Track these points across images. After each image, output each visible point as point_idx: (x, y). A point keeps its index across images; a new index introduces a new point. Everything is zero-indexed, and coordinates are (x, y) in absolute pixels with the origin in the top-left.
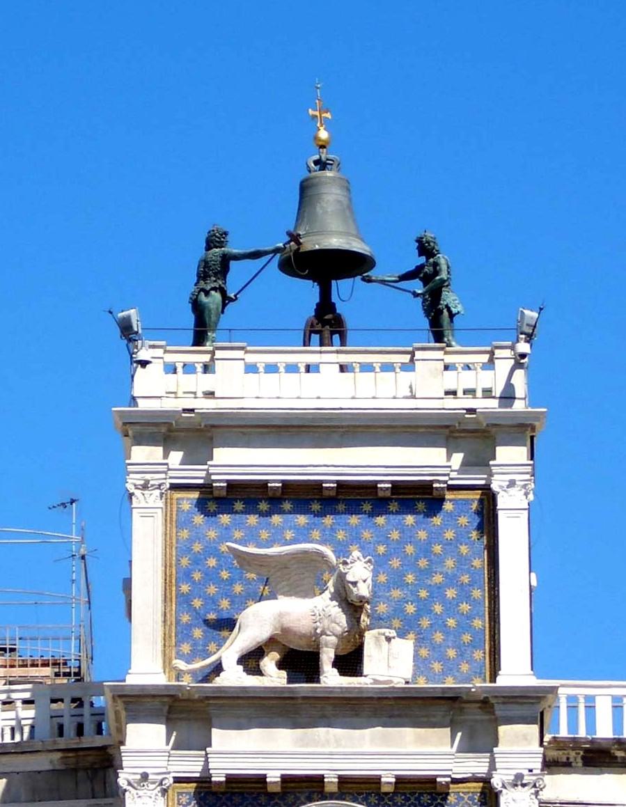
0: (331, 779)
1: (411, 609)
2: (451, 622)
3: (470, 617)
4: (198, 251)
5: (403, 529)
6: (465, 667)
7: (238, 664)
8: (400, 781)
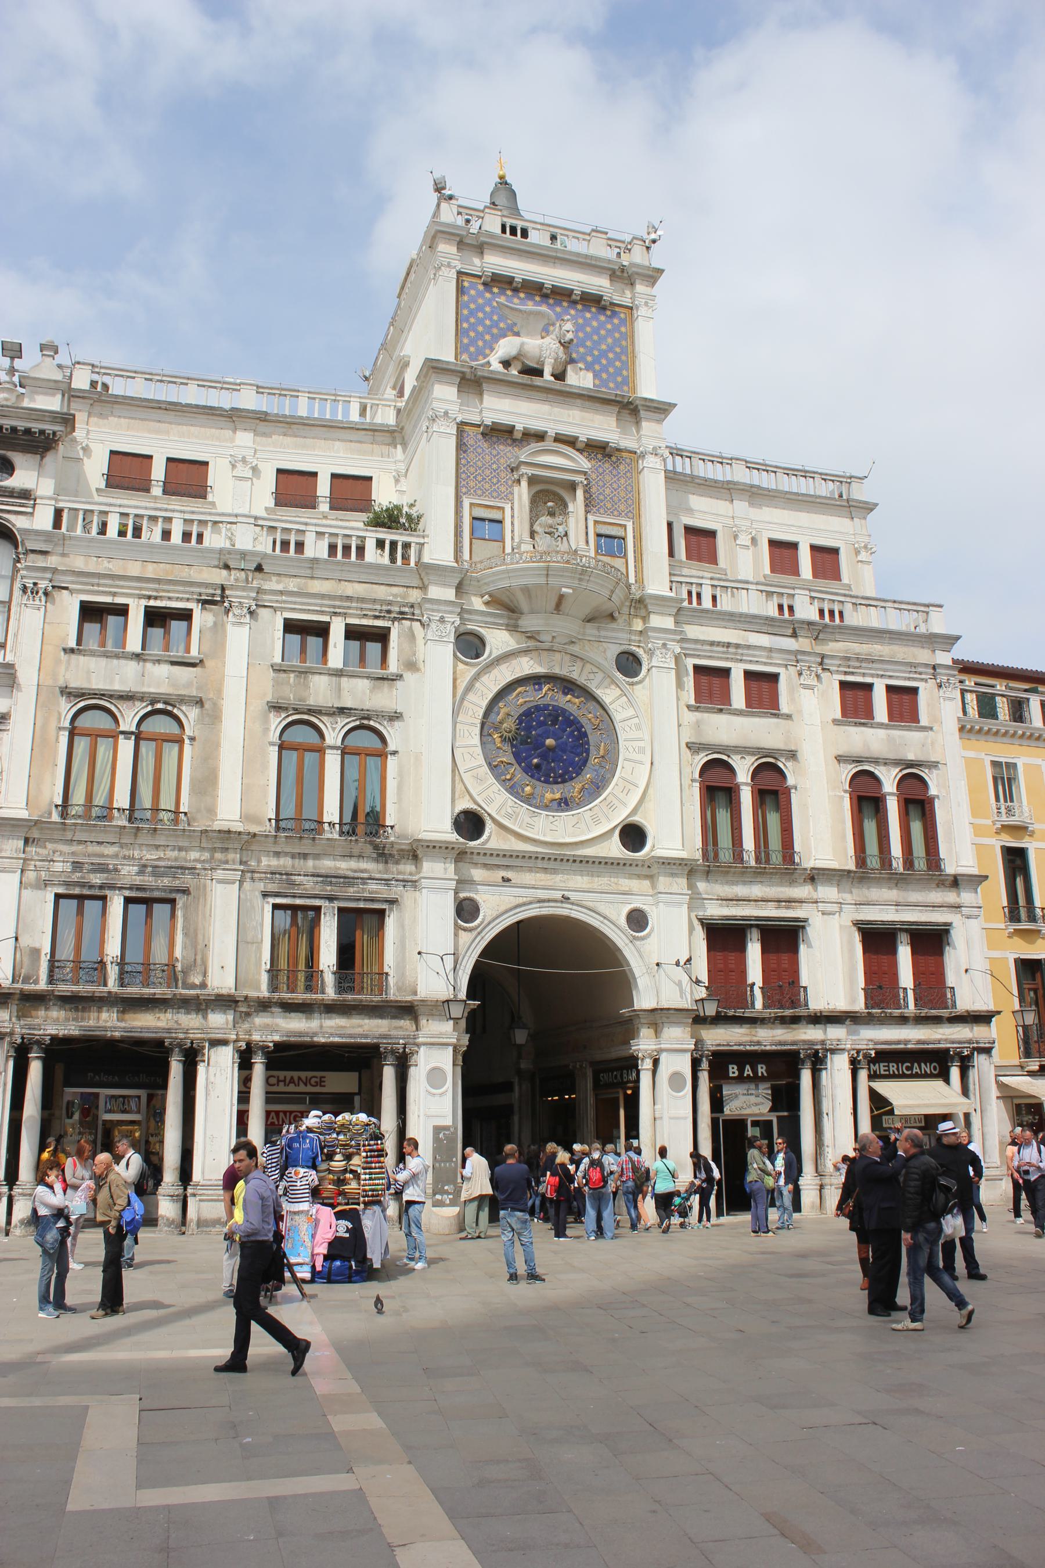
0: (551, 433)
2: (611, 370)
5: (585, 319)
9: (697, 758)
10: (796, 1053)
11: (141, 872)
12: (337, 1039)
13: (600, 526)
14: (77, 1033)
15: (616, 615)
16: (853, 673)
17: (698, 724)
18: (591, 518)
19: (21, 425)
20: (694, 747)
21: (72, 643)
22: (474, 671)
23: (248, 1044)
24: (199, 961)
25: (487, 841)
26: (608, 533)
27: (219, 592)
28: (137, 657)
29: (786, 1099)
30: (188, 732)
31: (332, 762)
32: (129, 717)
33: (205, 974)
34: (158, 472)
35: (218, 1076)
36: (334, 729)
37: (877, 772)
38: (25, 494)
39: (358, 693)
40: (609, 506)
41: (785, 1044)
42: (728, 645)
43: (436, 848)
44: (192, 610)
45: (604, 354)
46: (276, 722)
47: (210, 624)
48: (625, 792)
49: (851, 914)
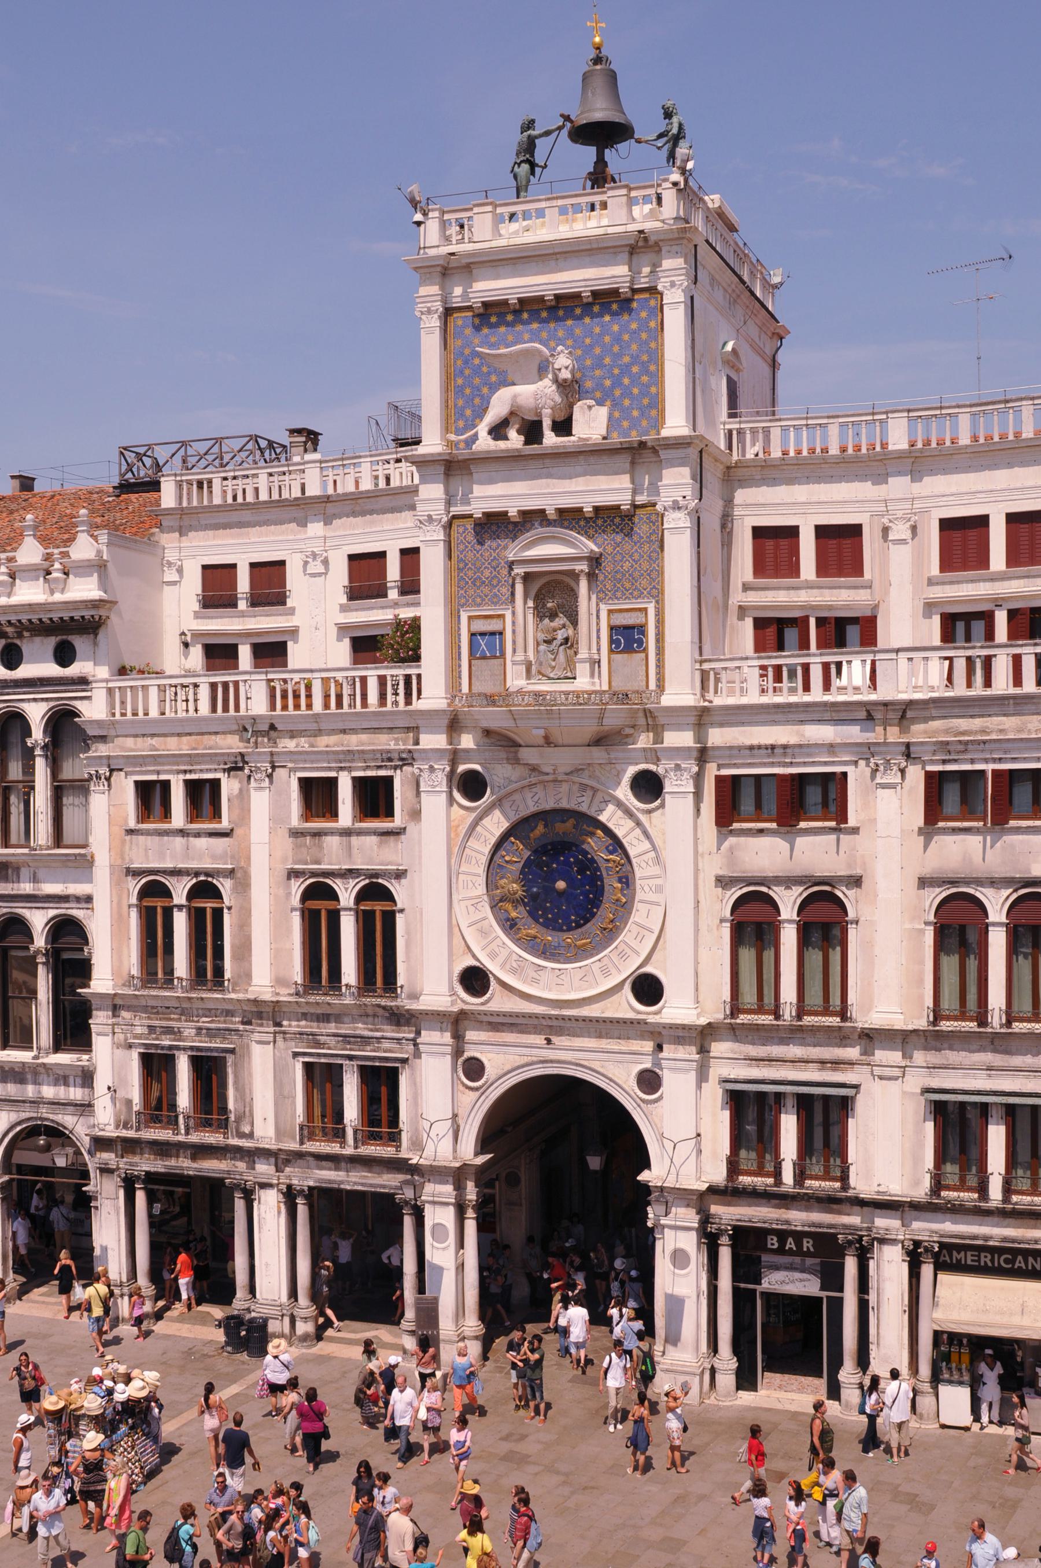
1: (608, 383)
2: (636, 391)
3: (648, 386)
4: (517, 138)
6: (644, 423)
7: (490, 433)
8: (597, 509)
9: (729, 893)
10: (834, 1236)
11: (198, 1034)
12: (360, 1188)
13: (616, 615)
14: (163, 1170)
15: (628, 731)
16: (955, 761)
17: (731, 850)
18: (604, 608)
19: (66, 616)
20: (723, 882)
21: (132, 824)
22: (474, 815)
23: (289, 1187)
24: (247, 1113)
25: (490, 999)
26: (625, 622)
27: (239, 758)
28: (181, 831)
29: (833, 1279)
30: (227, 901)
33: (253, 1126)
34: (243, 583)
36: (346, 889)
37: (978, 895)
38: (83, 681)
40: (628, 585)
41: (820, 1226)
42: (773, 747)
44: (219, 780)
45: (626, 369)
46: (297, 888)
47: (236, 791)
48: (639, 938)
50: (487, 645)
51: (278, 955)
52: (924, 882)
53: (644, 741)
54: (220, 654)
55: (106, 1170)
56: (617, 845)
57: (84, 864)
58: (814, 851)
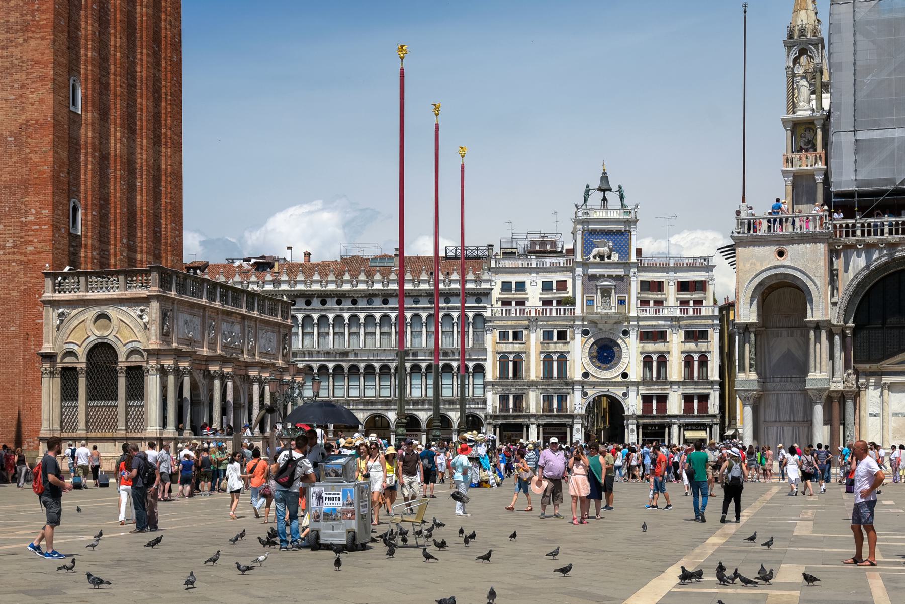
31: (555, 364)
32: (511, 357)
35: (533, 430)
38: (485, 308)
39: (560, 347)
43: (579, 383)
46: (542, 356)
49: (680, 392)
50: (590, 302)
51: (537, 371)
52: (682, 352)
53: (626, 324)
54: (506, 303)
55: (489, 424)
56: (618, 345)
57: (485, 351)
58: (660, 346)
